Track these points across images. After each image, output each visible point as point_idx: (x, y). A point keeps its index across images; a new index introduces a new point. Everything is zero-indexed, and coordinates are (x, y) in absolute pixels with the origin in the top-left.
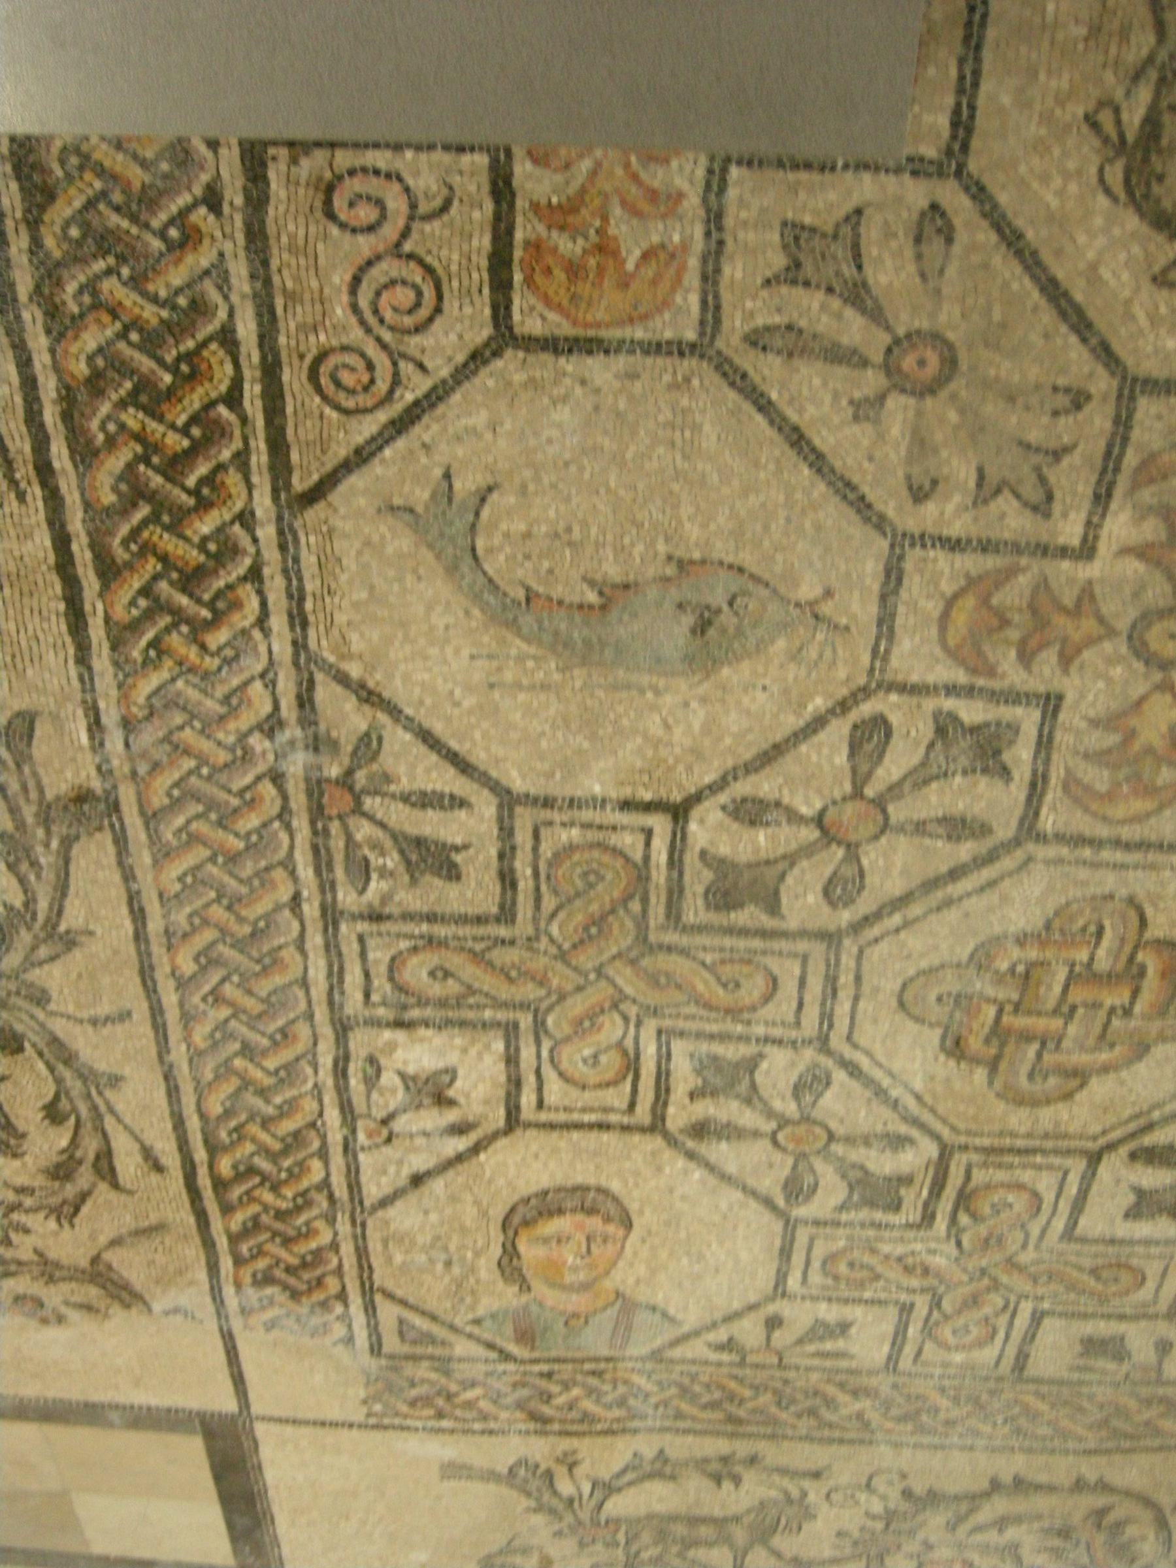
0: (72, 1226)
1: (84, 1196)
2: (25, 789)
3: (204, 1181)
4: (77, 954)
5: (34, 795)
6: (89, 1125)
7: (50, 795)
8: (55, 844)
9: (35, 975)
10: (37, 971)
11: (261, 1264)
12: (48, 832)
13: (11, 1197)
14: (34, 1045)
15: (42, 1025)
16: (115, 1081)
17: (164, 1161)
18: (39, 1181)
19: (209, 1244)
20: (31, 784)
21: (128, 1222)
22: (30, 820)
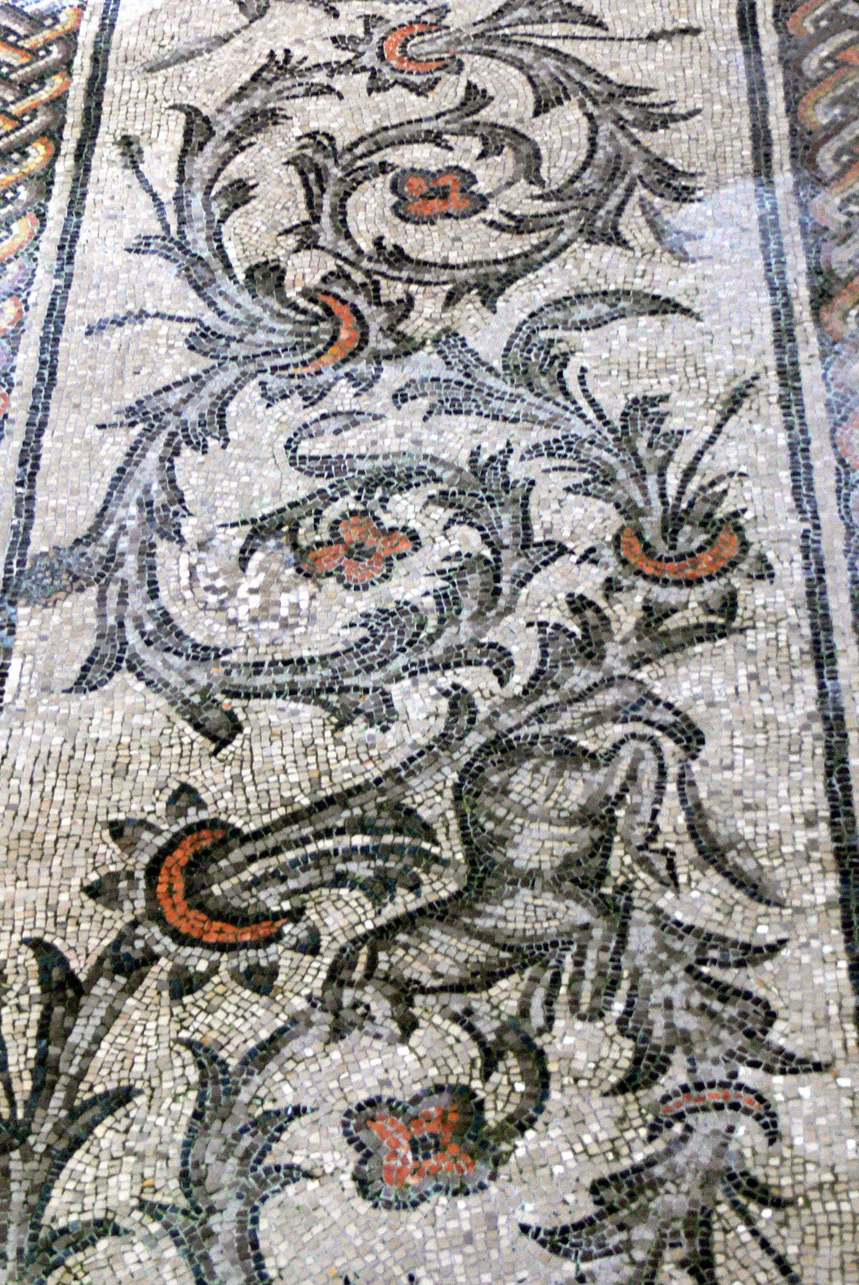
0: (272, 55)
1: (241, 94)
2: (123, 597)
3: (71, 136)
4: (130, 399)
5: (114, 589)
6: (196, 185)
7: (92, 592)
8: (110, 532)
9: (197, 365)
10: (193, 371)
11: (38, 39)
12: (114, 545)
13: (339, 82)
14: (233, 277)
15: (212, 304)
16: (143, 245)
17: (114, 153)
18: (290, 107)
19: (99, 59)
20: (112, 603)
21: (192, 69)
22: (131, 561)
